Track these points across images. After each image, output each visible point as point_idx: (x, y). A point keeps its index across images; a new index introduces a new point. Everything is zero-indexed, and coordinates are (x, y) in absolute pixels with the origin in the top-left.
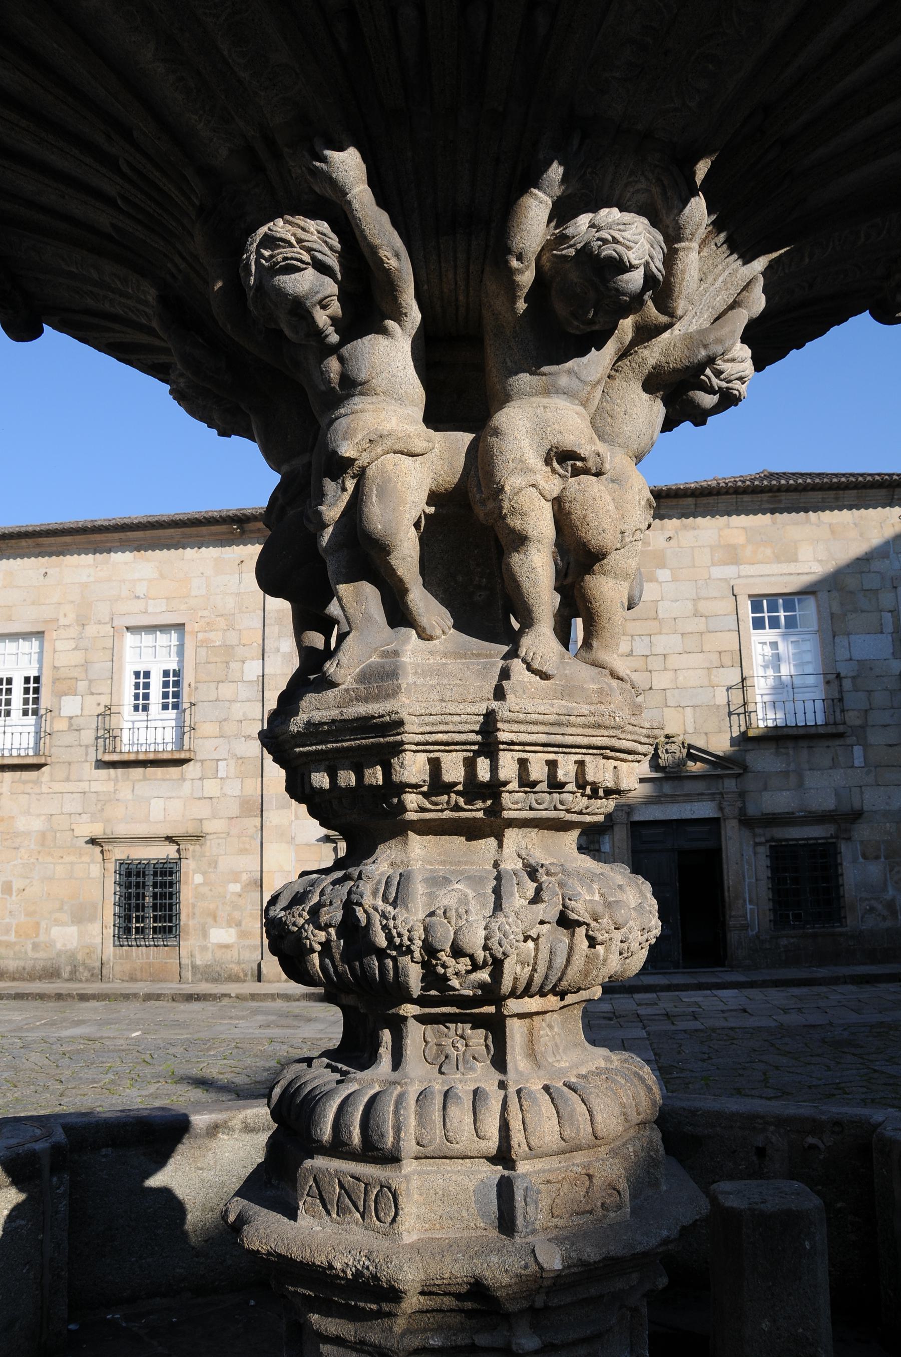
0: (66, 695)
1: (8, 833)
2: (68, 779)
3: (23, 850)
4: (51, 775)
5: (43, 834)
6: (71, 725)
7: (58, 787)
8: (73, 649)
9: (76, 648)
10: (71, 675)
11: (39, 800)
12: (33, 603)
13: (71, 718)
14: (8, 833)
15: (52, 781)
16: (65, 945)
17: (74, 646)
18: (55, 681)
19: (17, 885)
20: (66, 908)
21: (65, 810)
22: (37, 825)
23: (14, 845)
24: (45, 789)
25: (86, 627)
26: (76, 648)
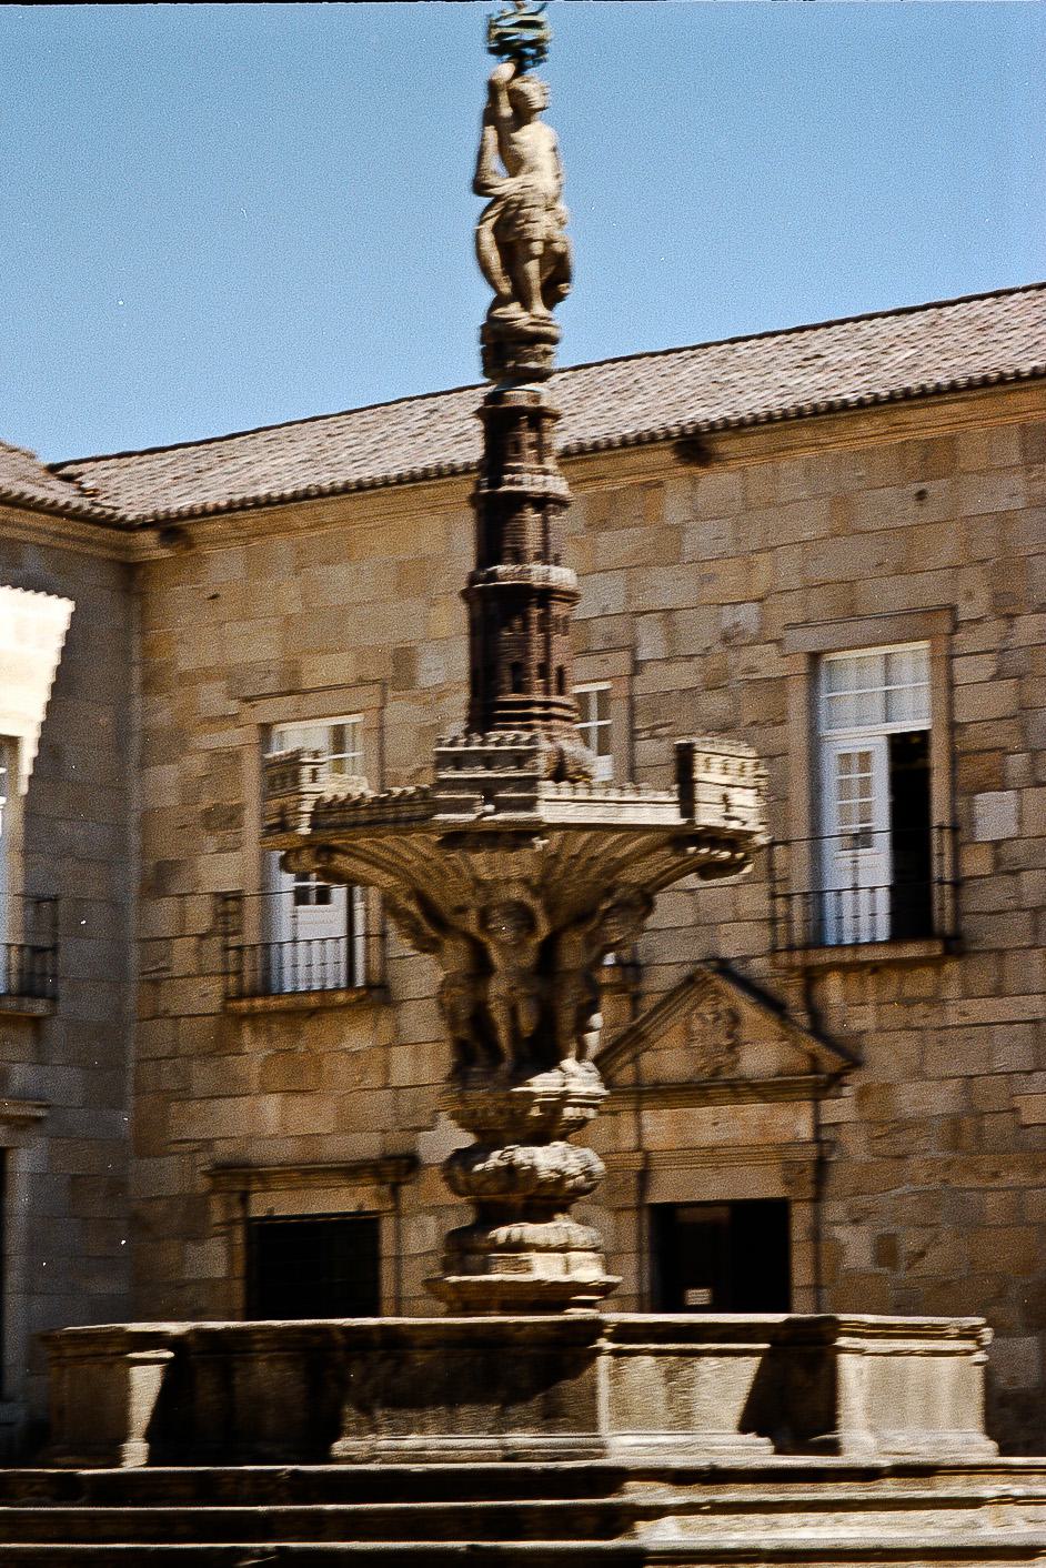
0: (983, 790)
1: (882, 1124)
2: (998, 992)
3: (914, 1161)
4: (964, 983)
5: (955, 1123)
6: (998, 862)
7: (981, 1009)
8: (993, 679)
9: (998, 676)
10: (988, 744)
11: (941, 1043)
12: (899, 571)
13: (997, 844)
14: (882, 1124)
15: (967, 996)
16: (1013, 1380)
17: (992, 671)
18: (955, 758)
19: (910, 1243)
20: (1013, 1293)
21: (998, 1065)
22: (939, 1100)
23: (898, 1150)
24: (953, 1019)
25: (1019, 621)
26: (998, 676)
